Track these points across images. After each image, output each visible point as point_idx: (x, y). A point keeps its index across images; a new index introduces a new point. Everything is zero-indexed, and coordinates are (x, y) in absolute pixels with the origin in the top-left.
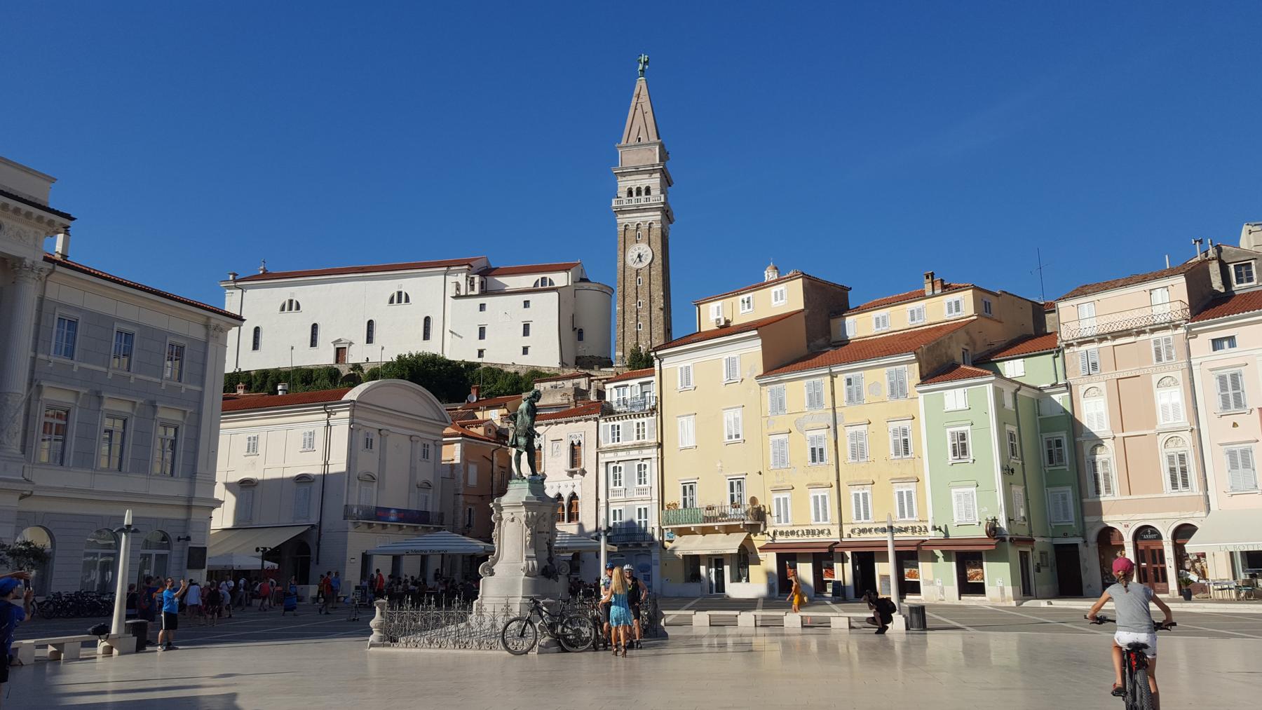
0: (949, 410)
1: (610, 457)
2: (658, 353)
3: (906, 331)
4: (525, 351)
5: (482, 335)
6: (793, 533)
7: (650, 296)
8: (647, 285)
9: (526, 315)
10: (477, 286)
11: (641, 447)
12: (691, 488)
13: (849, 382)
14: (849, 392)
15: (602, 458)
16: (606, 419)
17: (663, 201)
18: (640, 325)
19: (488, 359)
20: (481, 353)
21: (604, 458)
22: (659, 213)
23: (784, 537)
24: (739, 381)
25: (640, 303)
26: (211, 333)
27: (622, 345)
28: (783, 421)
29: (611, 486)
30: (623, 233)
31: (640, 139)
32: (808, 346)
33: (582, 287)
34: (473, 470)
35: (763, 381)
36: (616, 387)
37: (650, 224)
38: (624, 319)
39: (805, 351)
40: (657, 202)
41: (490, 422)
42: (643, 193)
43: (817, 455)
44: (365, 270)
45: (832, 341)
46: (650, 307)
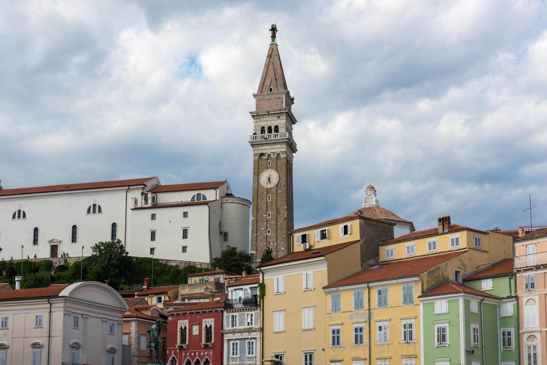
0: (437, 313)
2: (262, 269)
3: (425, 257)
4: (184, 249)
7: (277, 209)
8: (274, 201)
11: (250, 331)
13: (380, 293)
14: (380, 299)
16: (228, 311)
17: (287, 137)
18: (269, 231)
19: (155, 256)
22: (284, 146)
24: (313, 289)
25: (269, 214)
27: (255, 246)
28: (337, 318)
29: (231, 355)
30: (257, 161)
32: (362, 265)
33: (227, 200)
35: (327, 290)
36: (235, 290)
37: (277, 154)
38: (257, 227)
39: (359, 269)
40: (283, 138)
41: (155, 307)
42: (273, 131)
43: (358, 340)
44: (70, 189)
45: (380, 261)
46: (277, 217)
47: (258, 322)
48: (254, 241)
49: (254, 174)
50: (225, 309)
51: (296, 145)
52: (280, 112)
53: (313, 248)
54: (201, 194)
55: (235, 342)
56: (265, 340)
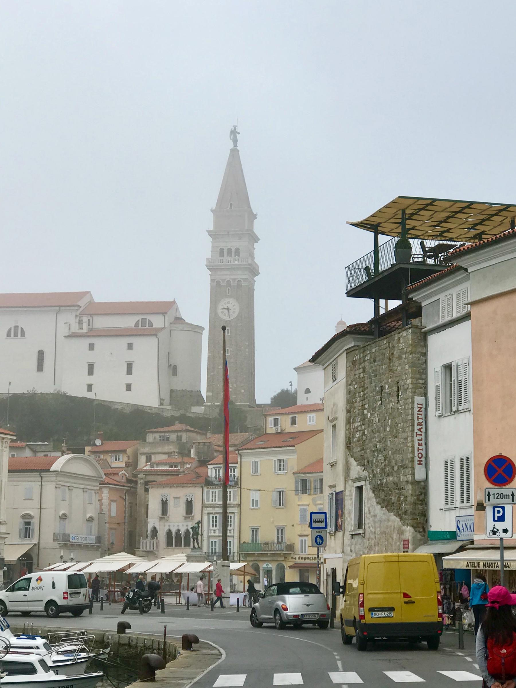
1: (210, 510)
2: (240, 452)
4: (129, 387)
5: (91, 370)
6: (308, 558)
9: (130, 356)
10: (85, 326)
12: (256, 531)
15: (206, 511)
20: (90, 388)
21: (206, 511)
23: (303, 561)
26: (4, 446)
29: (211, 527)
31: (231, 205)
34: (114, 506)
47: (236, 498)
48: (210, 381)
49: (211, 302)
50: (205, 485)
51: (258, 267)
52: (241, 233)
53: (284, 432)
54: (146, 319)
55: (214, 516)
56: (242, 514)
